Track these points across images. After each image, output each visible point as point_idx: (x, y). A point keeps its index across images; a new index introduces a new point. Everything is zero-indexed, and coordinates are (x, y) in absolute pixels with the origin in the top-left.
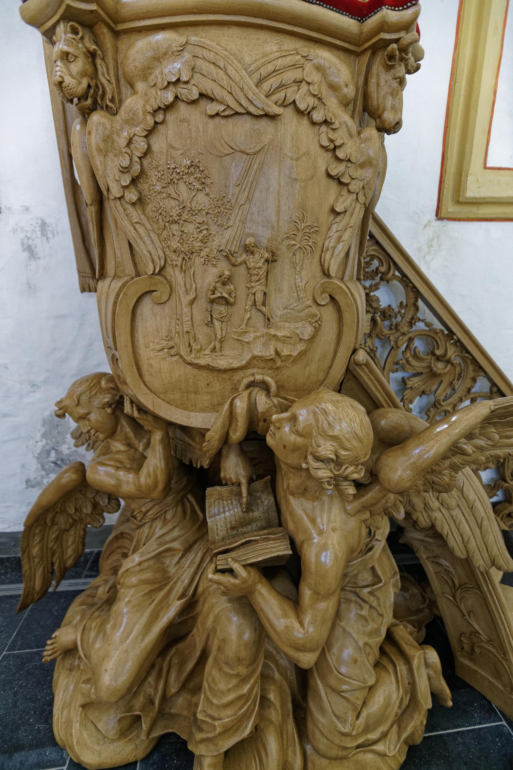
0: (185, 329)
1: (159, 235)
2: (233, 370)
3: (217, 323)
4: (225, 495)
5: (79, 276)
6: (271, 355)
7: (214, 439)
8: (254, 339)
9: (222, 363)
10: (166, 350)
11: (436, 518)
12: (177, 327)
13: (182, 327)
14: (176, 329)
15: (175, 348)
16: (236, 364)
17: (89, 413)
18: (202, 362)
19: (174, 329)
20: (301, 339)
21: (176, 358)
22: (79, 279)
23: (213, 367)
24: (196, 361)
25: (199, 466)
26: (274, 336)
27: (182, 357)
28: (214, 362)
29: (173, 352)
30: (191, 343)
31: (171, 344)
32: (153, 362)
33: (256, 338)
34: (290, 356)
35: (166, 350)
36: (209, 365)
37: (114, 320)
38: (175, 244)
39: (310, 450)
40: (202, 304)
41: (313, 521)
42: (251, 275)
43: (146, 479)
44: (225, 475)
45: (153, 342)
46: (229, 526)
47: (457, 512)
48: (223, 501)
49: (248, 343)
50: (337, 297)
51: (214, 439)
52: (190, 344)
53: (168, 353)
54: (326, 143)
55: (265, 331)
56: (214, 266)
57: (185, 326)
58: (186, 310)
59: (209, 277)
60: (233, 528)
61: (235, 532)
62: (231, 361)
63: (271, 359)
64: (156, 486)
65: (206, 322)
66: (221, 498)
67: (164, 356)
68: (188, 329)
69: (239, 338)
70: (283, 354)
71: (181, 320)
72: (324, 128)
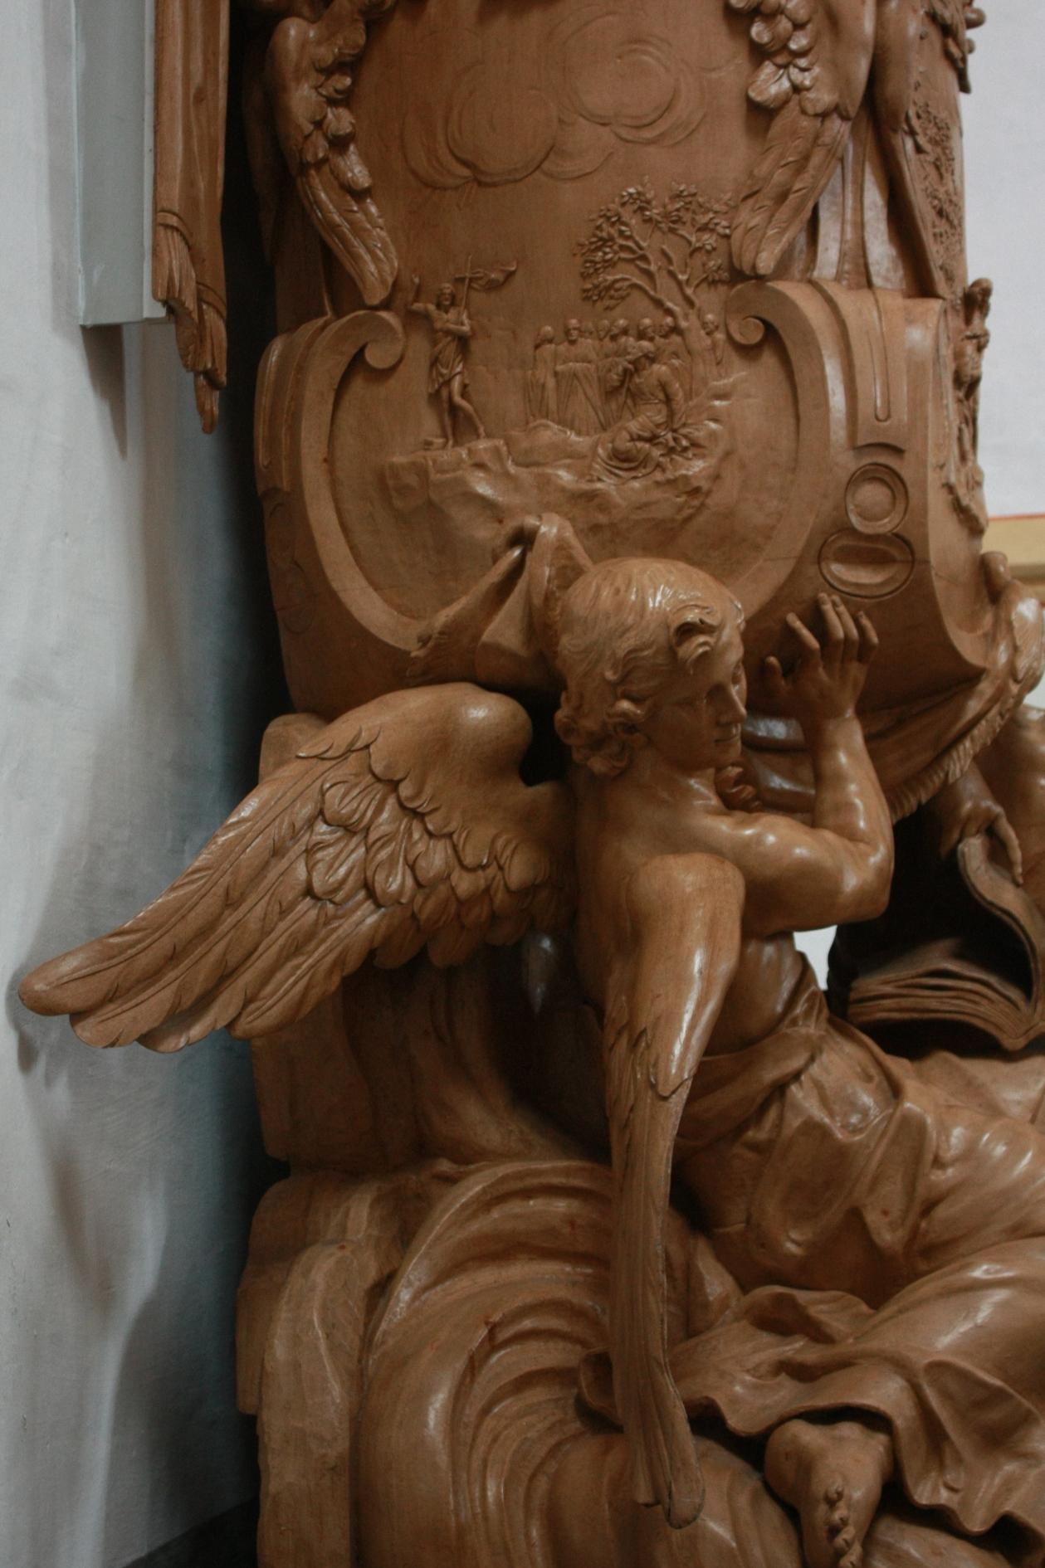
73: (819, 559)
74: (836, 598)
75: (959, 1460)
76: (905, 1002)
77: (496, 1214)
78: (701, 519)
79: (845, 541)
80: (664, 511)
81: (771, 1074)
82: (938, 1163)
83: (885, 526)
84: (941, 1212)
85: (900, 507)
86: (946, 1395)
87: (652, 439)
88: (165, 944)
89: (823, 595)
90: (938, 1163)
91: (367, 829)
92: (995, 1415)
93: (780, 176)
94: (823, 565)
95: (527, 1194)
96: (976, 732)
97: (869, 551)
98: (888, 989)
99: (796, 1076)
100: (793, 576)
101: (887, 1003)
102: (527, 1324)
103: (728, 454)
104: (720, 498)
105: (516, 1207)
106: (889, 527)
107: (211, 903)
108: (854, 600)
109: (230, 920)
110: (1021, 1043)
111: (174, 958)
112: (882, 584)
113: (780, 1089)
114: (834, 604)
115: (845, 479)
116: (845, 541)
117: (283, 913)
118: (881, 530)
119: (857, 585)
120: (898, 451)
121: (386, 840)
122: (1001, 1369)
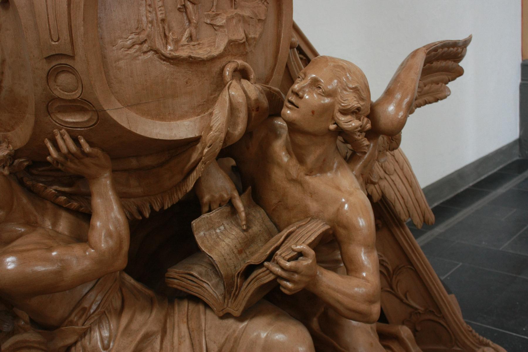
0: (160, 17)
2: (213, 59)
4: (216, 220)
6: (243, 38)
7: (218, 141)
8: (226, 21)
9: (202, 53)
10: (137, 47)
11: (384, 186)
12: (149, 15)
13: (156, 14)
14: (147, 18)
15: (149, 41)
18: (184, 53)
19: (144, 19)
20: (259, 20)
21: (150, 54)
23: (195, 58)
24: (177, 54)
25: (147, 215)
26: (243, 17)
27: (156, 52)
28: (194, 52)
29: (145, 46)
30: (167, 33)
31: (143, 36)
32: (122, 63)
33: (229, 19)
34: (254, 38)
35: (137, 47)
36: (190, 57)
37: (69, 14)
39: (337, 107)
41: (338, 188)
43: (107, 242)
44: (213, 196)
45: (121, 38)
46: (236, 251)
47: (395, 177)
48: (215, 229)
49: (221, 27)
51: (218, 141)
52: (165, 34)
53: (139, 50)
55: (232, 12)
57: (159, 13)
60: (240, 252)
61: (244, 255)
62: (209, 49)
63: (244, 42)
64: (121, 248)
65: (179, 6)
66: (212, 226)
67: (136, 54)
68: (163, 16)
69: (213, 22)
70: (250, 36)
71: (153, 6)
74: (63, 131)
79: (58, 104)
83: (76, 95)
85: (80, 86)
89: (56, 131)
94: (53, 117)
96: (197, 168)
98: (176, 276)
99: (75, 343)
100: (36, 122)
101: (176, 281)
106: (78, 95)
110: (221, 314)
112: (88, 121)
114: (62, 135)
115: (45, 76)
116: (58, 104)
118: (75, 97)
119: (74, 123)
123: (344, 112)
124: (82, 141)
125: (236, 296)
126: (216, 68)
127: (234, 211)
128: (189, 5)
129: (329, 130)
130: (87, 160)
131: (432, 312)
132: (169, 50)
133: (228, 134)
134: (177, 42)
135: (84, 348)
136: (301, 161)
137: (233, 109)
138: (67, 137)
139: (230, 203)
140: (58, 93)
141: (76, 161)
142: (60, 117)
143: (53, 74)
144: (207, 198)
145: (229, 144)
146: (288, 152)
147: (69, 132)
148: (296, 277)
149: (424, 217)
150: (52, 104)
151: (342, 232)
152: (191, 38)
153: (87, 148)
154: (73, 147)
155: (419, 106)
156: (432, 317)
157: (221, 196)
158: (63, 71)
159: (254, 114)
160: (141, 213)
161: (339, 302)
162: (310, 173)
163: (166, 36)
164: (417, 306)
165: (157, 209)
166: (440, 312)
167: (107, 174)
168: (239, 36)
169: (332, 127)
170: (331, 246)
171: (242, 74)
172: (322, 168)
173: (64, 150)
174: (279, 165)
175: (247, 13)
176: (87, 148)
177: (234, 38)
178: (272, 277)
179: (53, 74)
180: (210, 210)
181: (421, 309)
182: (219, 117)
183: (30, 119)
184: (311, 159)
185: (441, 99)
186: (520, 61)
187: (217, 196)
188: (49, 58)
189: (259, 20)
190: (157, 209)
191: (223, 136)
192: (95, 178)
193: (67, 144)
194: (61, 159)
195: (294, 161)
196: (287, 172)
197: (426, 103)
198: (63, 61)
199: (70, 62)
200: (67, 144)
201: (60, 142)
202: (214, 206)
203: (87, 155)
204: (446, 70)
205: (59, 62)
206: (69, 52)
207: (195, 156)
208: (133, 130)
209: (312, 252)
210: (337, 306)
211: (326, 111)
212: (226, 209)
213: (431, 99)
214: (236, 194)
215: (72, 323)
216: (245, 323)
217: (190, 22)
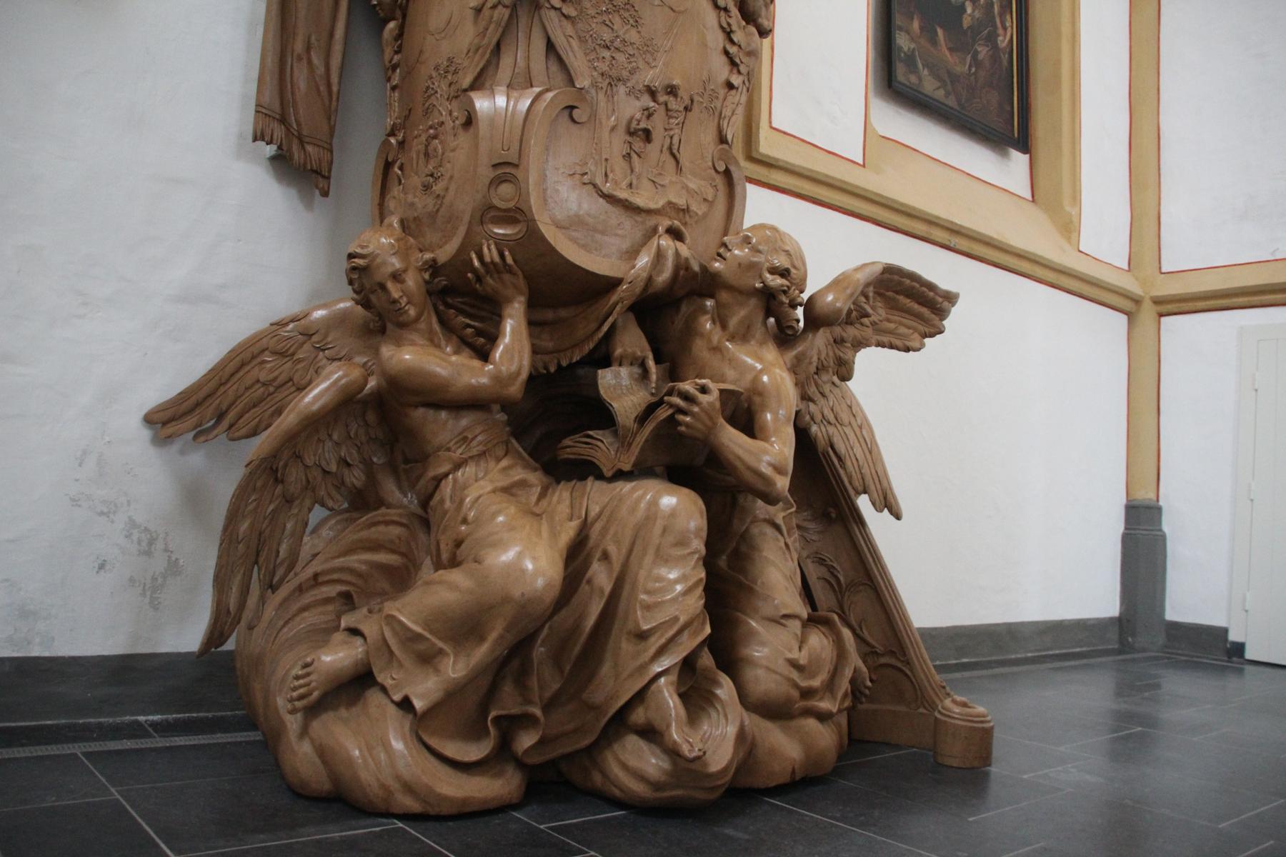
1: (586, 54)
3: (634, 156)
5: (257, 112)
9: (640, 201)
16: (653, 206)
17: (405, 271)
18: (622, 194)
22: (255, 118)
25: (552, 370)
27: (595, 186)
38: (604, 67)
40: (621, 136)
42: (670, 117)
47: (848, 430)
49: (662, 186)
50: (732, 168)
54: (725, 25)
56: (638, 98)
58: (606, 134)
59: (630, 107)
72: (722, 13)
73: (482, 223)
75: (401, 665)
76: (574, 450)
77: (373, 529)
78: (443, 210)
80: (430, 208)
81: (431, 473)
82: (465, 521)
84: (463, 546)
86: (395, 633)
87: (432, 175)
88: (193, 400)
90: (465, 521)
91: (293, 354)
92: (421, 647)
93: (476, 41)
95: (387, 523)
97: (509, 217)
99: (446, 475)
102: (335, 576)
103: (451, 177)
104: (447, 200)
105: (381, 528)
107: (213, 384)
108: (500, 243)
109: (222, 389)
111: (198, 405)
113: (439, 480)
117: (247, 389)
120: (516, 166)
121: (300, 361)
122: (426, 625)
123: (774, 271)
124: (507, 253)
125: (630, 445)
126: (651, 221)
127: (645, 374)
128: (634, 156)
129: (756, 289)
130: (507, 277)
131: (892, 653)
132: (607, 188)
133: (650, 279)
134: (616, 183)
135: (455, 480)
136: (724, 327)
137: (659, 256)
138: (493, 247)
139: (643, 365)
140: (496, 202)
141: (496, 276)
142: (490, 226)
143: (497, 182)
144: (619, 351)
145: (651, 291)
146: (714, 322)
147: (496, 244)
148: (696, 409)
149: (885, 498)
150: (488, 213)
151: (757, 399)
152: (630, 185)
153: (509, 260)
154: (497, 259)
155: (880, 344)
156: (893, 661)
157: (634, 353)
158: (506, 181)
159: (682, 273)
160: (546, 368)
161: (739, 458)
162: (732, 338)
163: (606, 175)
164: (874, 643)
165: (564, 364)
166: (905, 655)
167: (522, 299)
168: (681, 202)
169: (758, 285)
170: (743, 414)
171: (675, 234)
172: (742, 336)
173: (487, 259)
174: (702, 335)
175: (692, 186)
176: (509, 260)
177: (674, 200)
178: (670, 412)
179: (497, 182)
180: (620, 365)
181: (880, 649)
182: (644, 260)
183: (462, 231)
184: (733, 322)
185: (915, 350)
186: (1124, 501)
187: (630, 350)
188: (495, 166)
189: (705, 200)
190: (564, 364)
191: (645, 275)
192: (509, 301)
193: (491, 253)
194: (482, 270)
195: (718, 329)
196: (710, 341)
197: (892, 347)
198: (507, 170)
199: (513, 171)
200: (491, 253)
201: (485, 250)
202: (625, 361)
203: (509, 270)
204: (919, 316)
205: (506, 170)
206: (516, 161)
207: (614, 298)
208: (558, 248)
209: (716, 394)
210: (738, 464)
211: (752, 267)
212: (637, 370)
213: (898, 343)
214: (650, 356)
215: (449, 450)
216: (633, 484)
217: (632, 171)
